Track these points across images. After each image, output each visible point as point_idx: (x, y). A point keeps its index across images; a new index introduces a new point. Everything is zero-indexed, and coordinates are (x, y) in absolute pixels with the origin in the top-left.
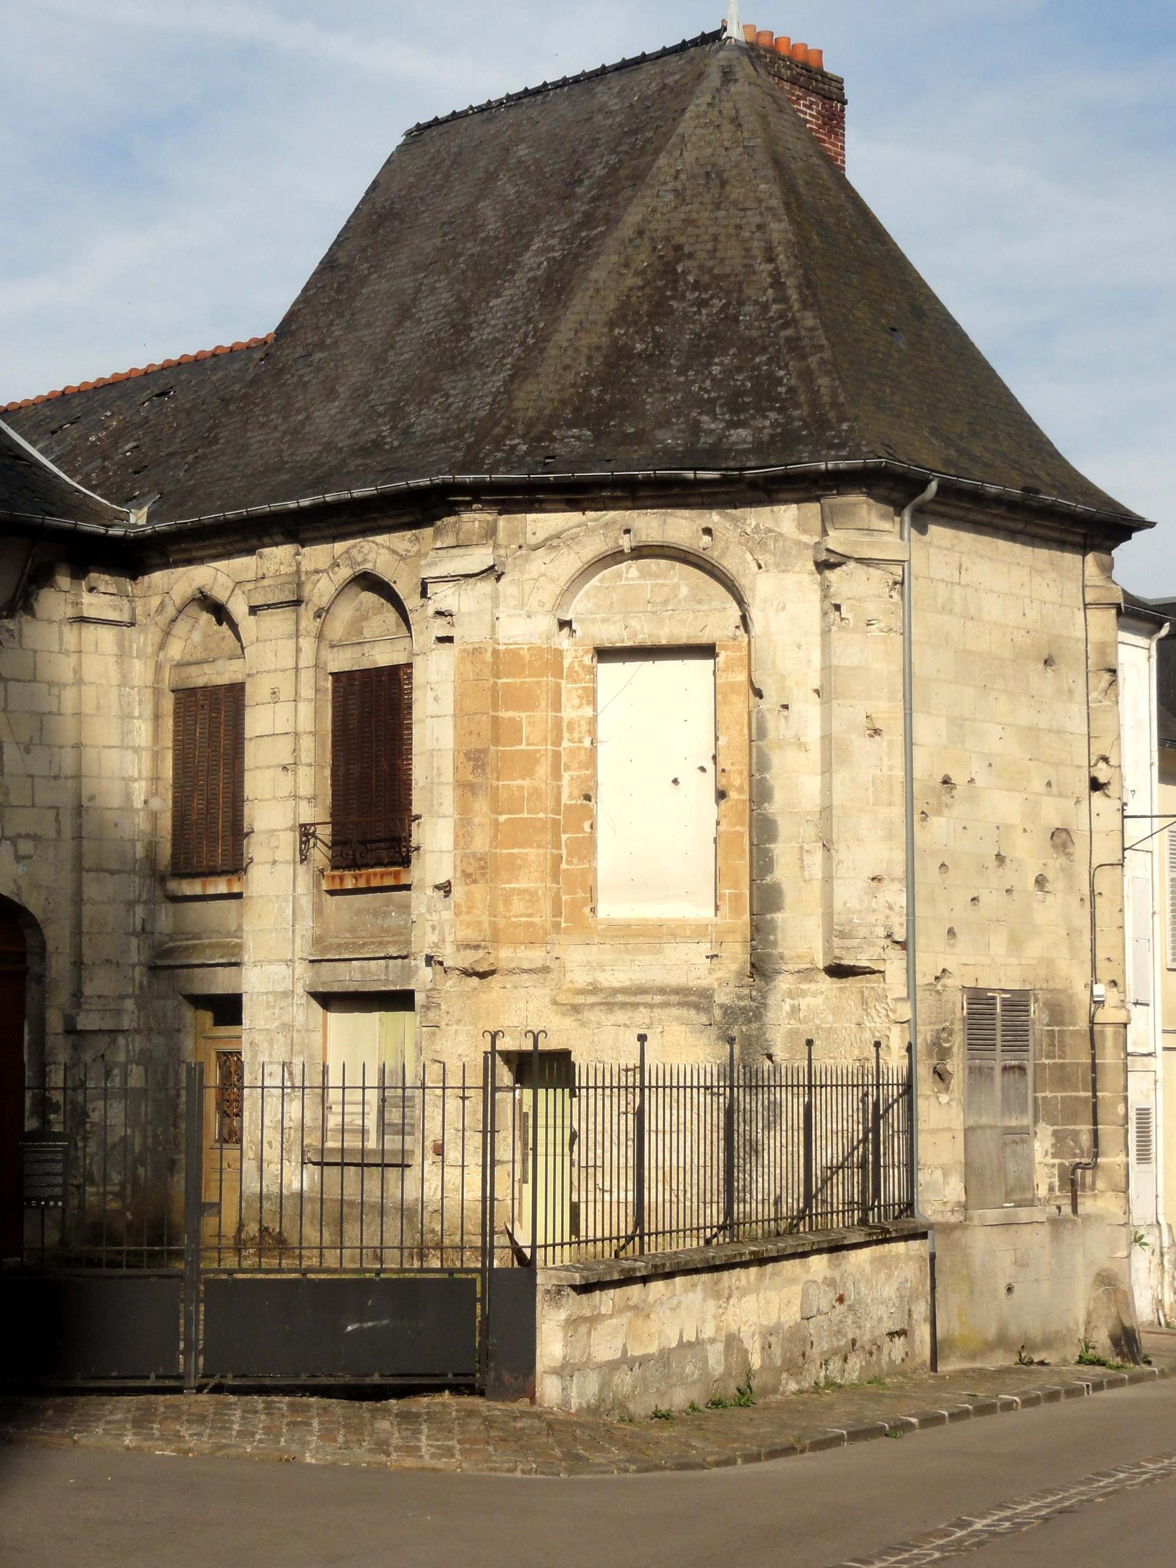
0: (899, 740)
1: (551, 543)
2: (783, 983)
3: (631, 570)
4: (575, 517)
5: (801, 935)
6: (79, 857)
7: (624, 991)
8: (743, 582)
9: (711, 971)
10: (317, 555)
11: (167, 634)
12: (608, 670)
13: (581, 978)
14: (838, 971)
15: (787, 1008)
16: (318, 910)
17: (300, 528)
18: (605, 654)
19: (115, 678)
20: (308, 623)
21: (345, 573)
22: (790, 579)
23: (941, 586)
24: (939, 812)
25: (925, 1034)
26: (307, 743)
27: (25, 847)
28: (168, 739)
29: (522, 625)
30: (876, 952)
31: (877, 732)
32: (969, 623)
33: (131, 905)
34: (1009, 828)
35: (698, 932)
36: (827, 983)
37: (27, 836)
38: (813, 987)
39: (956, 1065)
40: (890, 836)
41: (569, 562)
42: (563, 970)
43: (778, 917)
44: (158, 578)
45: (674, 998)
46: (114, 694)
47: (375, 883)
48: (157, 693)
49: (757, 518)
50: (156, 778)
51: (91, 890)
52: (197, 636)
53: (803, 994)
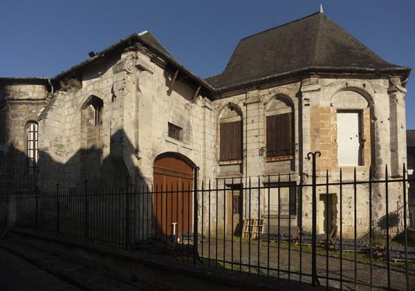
1: (330, 85)
4: (335, 80)
6: (205, 155)
10: (265, 92)
11: (220, 112)
12: (339, 115)
16: (265, 166)
17: (259, 86)
18: (340, 111)
20: (262, 105)
21: (273, 94)
22: (382, 95)
26: (262, 131)
28: (219, 134)
29: (324, 103)
44: (218, 101)
47: (281, 159)
48: (217, 124)
49: (375, 82)
50: (217, 141)
51: (207, 163)
52: (226, 113)
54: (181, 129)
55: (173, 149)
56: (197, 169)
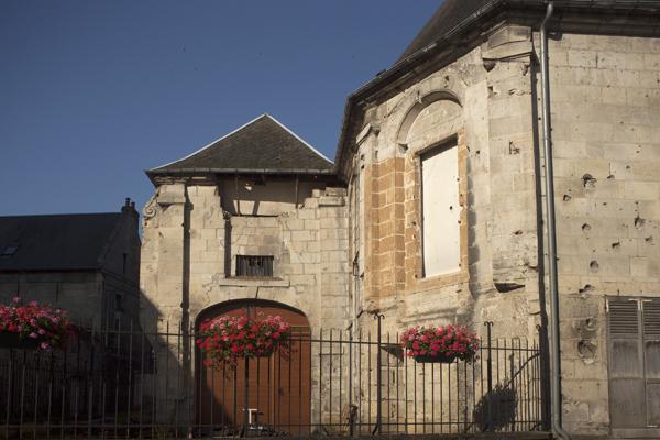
0: (531, 152)
2: (482, 299)
3: (425, 112)
4: (401, 95)
5: (486, 275)
7: (427, 314)
8: (460, 96)
9: (459, 298)
13: (411, 310)
14: (503, 288)
15: (482, 312)
19: (336, 225)
23: (579, 71)
24: (581, 195)
25: (568, 322)
27: (301, 289)
30: (519, 274)
31: (517, 150)
32: (606, 90)
33: (344, 307)
34: (647, 203)
35: (454, 277)
36: (499, 296)
37: (302, 285)
38: (494, 299)
39: (600, 340)
40: (526, 207)
41: (400, 115)
42: (405, 307)
43: (477, 264)
45: (442, 314)
46: (336, 231)
53: (488, 305)
54: (272, 257)
55: (242, 294)
56: (303, 314)
